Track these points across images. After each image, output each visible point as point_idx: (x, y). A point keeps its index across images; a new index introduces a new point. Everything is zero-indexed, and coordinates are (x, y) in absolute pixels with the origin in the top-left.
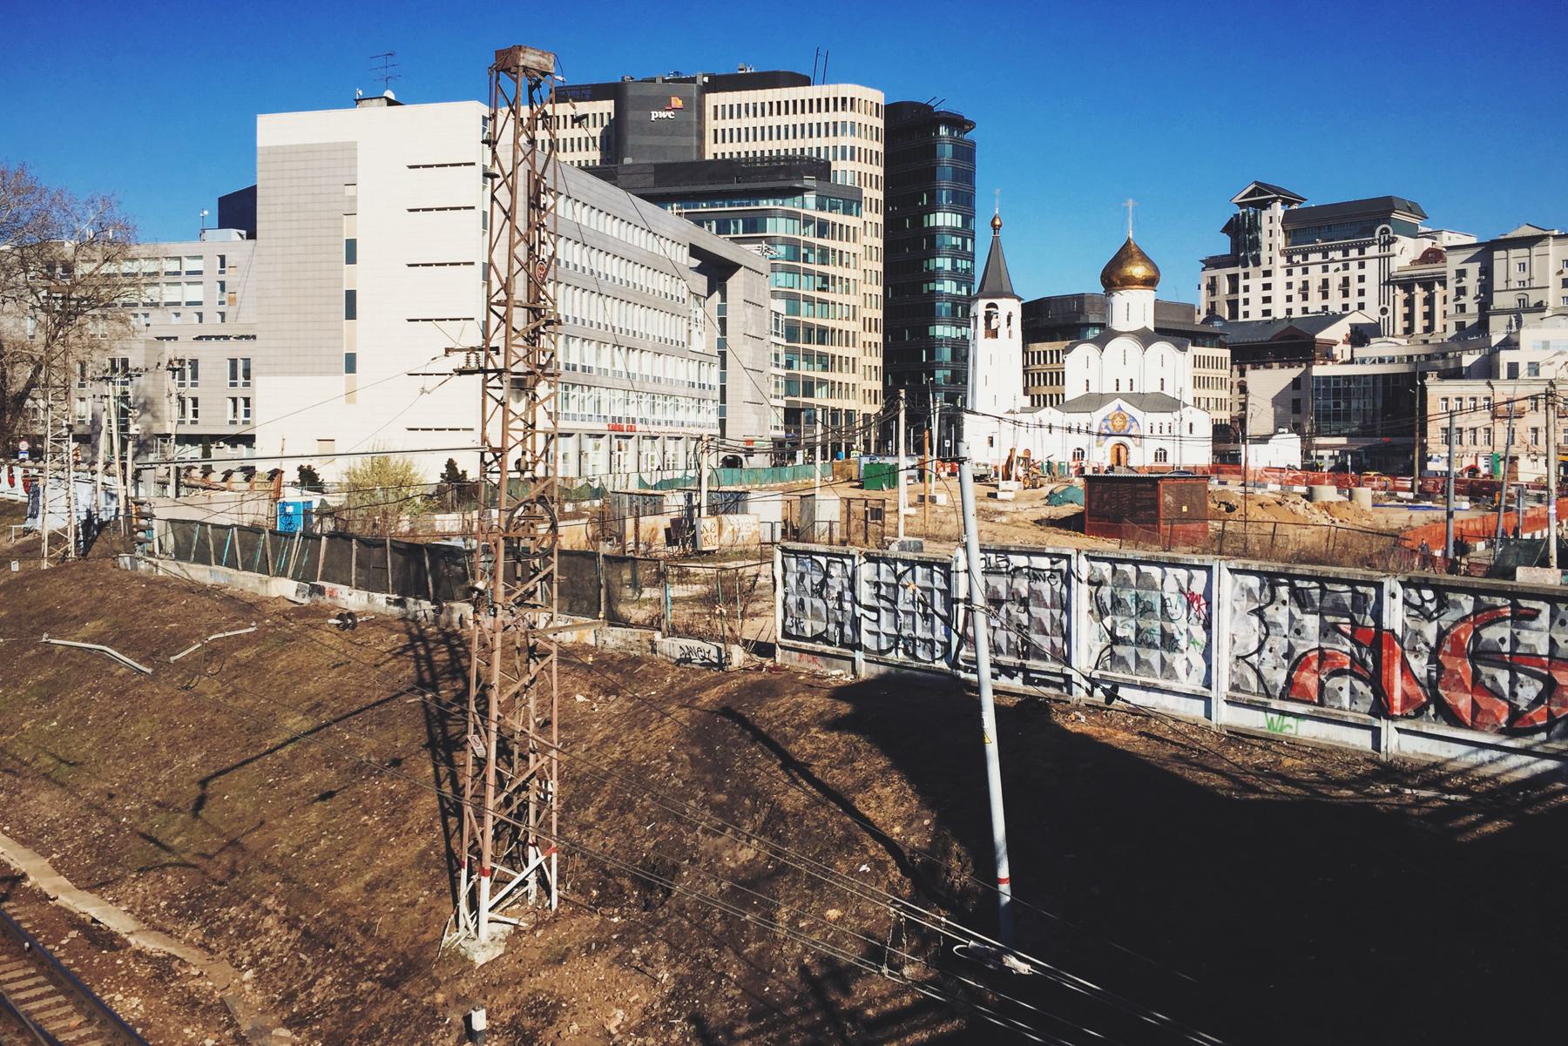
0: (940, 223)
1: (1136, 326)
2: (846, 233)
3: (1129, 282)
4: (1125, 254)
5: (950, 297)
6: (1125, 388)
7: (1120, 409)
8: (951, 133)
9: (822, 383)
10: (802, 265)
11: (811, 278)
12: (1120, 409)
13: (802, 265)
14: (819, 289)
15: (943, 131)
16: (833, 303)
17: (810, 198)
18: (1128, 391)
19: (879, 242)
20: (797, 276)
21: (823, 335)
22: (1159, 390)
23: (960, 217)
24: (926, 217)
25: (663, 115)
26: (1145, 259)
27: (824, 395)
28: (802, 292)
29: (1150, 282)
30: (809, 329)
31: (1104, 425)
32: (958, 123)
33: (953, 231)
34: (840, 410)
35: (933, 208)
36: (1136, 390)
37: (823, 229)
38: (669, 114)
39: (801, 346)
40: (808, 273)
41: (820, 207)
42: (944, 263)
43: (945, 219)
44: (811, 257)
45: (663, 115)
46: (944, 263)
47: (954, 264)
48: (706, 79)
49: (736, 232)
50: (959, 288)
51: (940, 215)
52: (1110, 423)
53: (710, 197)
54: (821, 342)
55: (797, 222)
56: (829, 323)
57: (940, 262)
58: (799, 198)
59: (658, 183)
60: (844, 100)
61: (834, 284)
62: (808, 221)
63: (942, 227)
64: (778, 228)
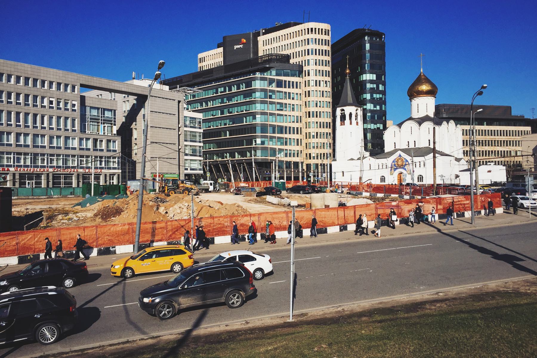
0: (364, 79)
1: (422, 114)
2: (296, 85)
3: (421, 93)
4: (419, 81)
5: (371, 111)
6: (412, 146)
7: (400, 156)
8: (371, 39)
9: (281, 150)
10: (269, 100)
11: (274, 105)
12: (400, 156)
13: (269, 100)
14: (278, 110)
15: (366, 38)
16: (286, 115)
17: (274, 72)
18: (413, 147)
19: (329, 89)
20: (266, 105)
21: (282, 129)
22: (428, 145)
23: (375, 75)
24: (359, 77)
25: (238, 47)
26: (428, 81)
27: (283, 156)
28: (268, 111)
29: (432, 93)
30: (274, 127)
31: (393, 163)
32: (376, 34)
33: (371, 82)
34: (291, 162)
35: (363, 72)
36: (416, 147)
37: (280, 84)
38: (241, 46)
39: (269, 135)
40: (271, 103)
41: (277, 75)
42: (368, 96)
43: (368, 77)
44: (273, 96)
45: (238, 47)
46: (368, 96)
47: (372, 96)
48: (264, 31)
49: (243, 88)
50: (375, 107)
51: (364, 75)
52: (396, 163)
53: (235, 76)
54: (282, 133)
55: (266, 82)
56: (284, 124)
57: (365, 96)
58: (269, 71)
59: (225, 72)
60: (312, 29)
61: (286, 107)
62: (271, 82)
63: (366, 80)
64: (257, 84)
